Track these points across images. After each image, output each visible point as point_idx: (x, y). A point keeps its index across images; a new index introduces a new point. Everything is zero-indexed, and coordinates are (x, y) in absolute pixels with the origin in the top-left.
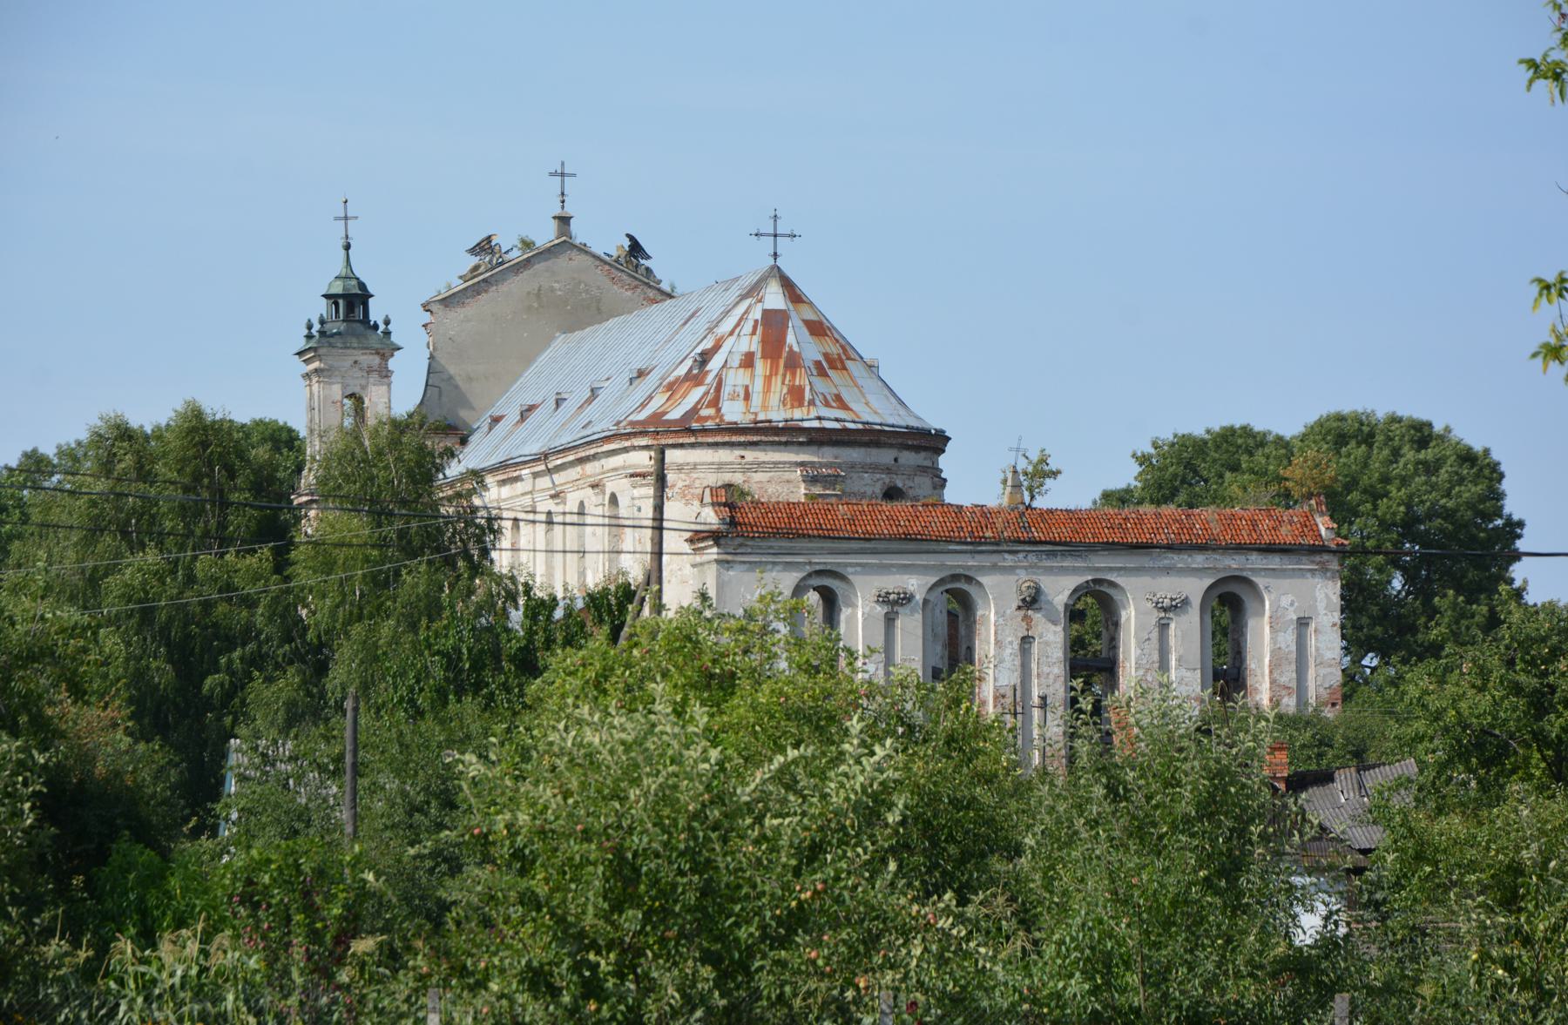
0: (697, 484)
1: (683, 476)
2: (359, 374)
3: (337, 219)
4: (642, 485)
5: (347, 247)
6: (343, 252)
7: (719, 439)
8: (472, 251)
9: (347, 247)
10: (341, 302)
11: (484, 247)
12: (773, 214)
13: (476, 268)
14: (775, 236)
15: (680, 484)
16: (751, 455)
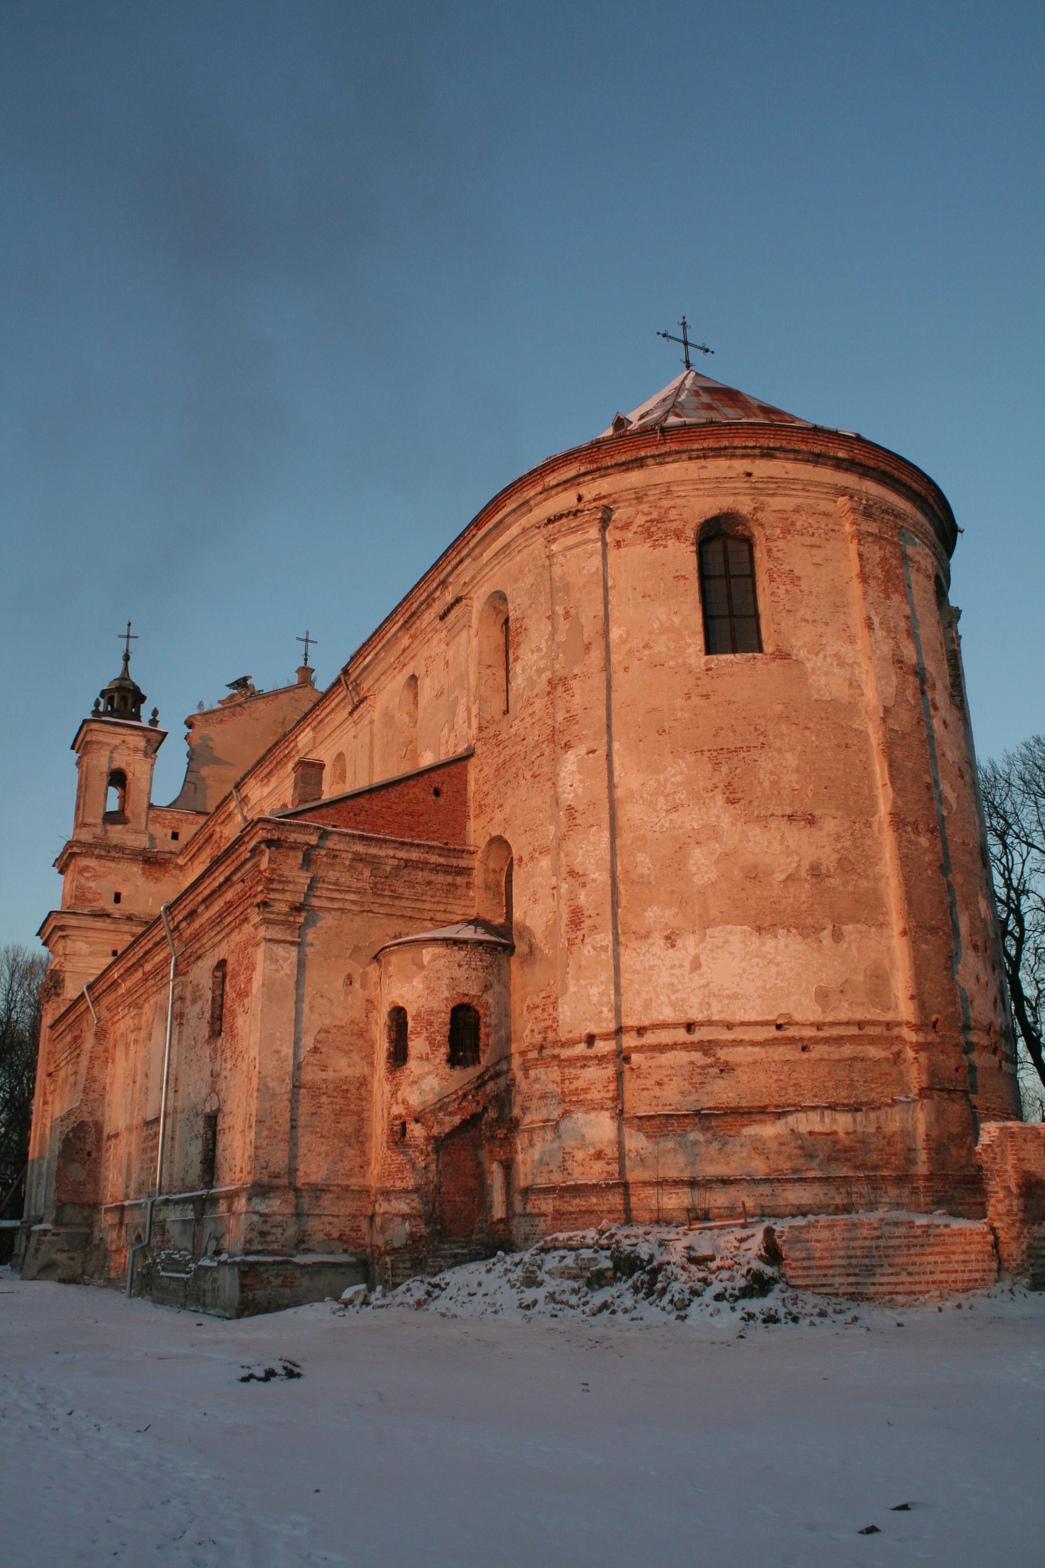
0: (673, 514)
1: (645, 507)
2: (126, 752)
3: (120, 636)
4: (573, 531)
5: (127, 658)
6: (123, 662)
7: (711, 443)
8: (231, 686)
9: (127, 658)
10: (116, 696)
11: (242, 683)
12: (682, 321)
13: (231, 697)
14: (686, 343)
15: (641, 519)
16: (763, 468)
